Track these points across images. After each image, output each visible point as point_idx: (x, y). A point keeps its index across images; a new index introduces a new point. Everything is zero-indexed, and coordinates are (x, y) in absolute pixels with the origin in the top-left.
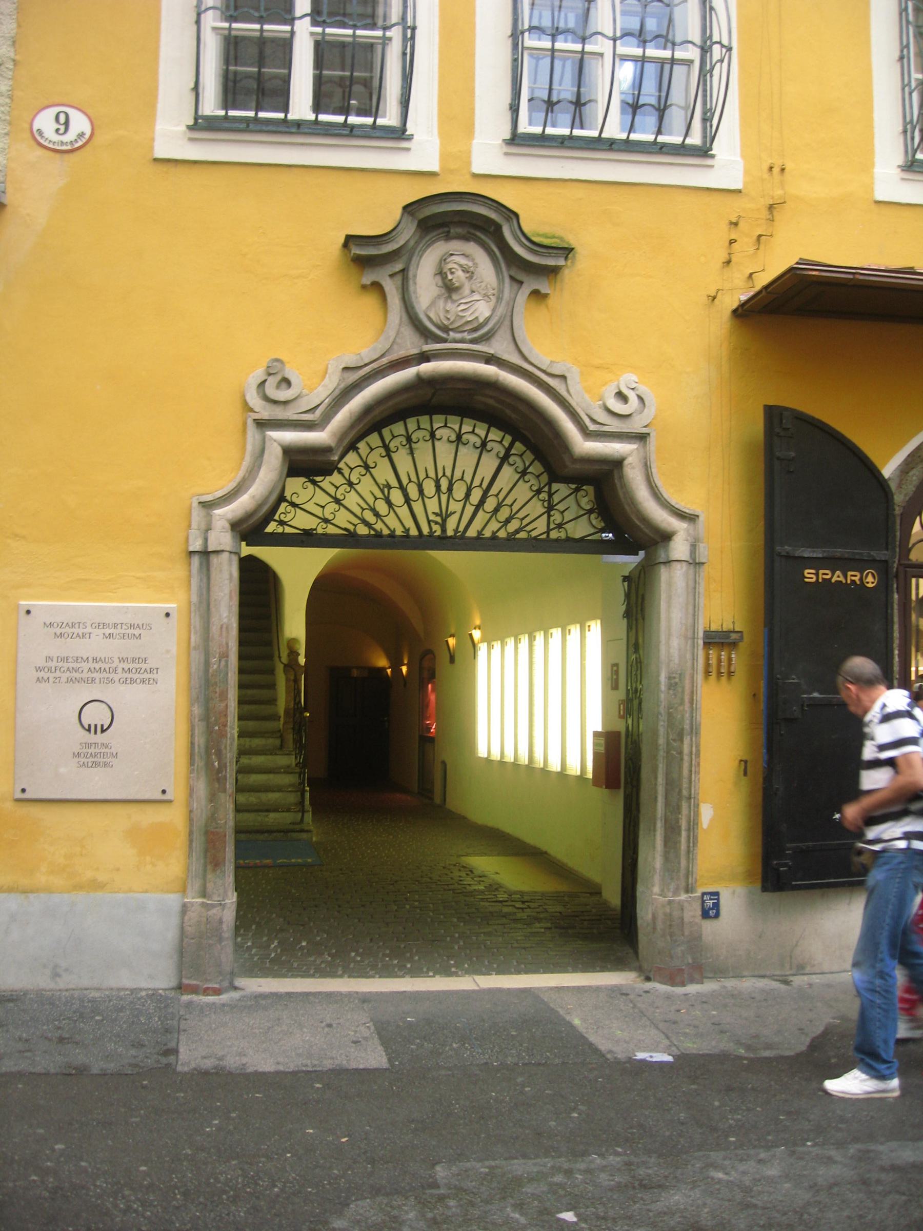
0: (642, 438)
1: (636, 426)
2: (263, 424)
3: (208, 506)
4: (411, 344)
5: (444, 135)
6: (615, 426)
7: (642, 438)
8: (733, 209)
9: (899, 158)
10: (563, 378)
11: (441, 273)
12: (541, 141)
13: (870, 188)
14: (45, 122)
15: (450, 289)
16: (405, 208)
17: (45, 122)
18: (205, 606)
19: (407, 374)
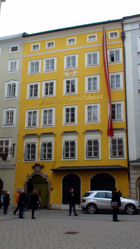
0: (47, 177)
1: (47, 176)
2: (28, 177)
3: (25, 182)
4: (35, 172)
5: (38, 160)
6: (46, 176)
7: (47, 177)
8: (53, 162)
9: (63, 158)
10: (43, 173)
11: (37, 168)
12: (42, 160)
13: (61, 160)
14: (18, 161)
15: (37, 169)
16: (35, 165)
17: (18, 161)
18: (24, 187)
19: (34, 174)
